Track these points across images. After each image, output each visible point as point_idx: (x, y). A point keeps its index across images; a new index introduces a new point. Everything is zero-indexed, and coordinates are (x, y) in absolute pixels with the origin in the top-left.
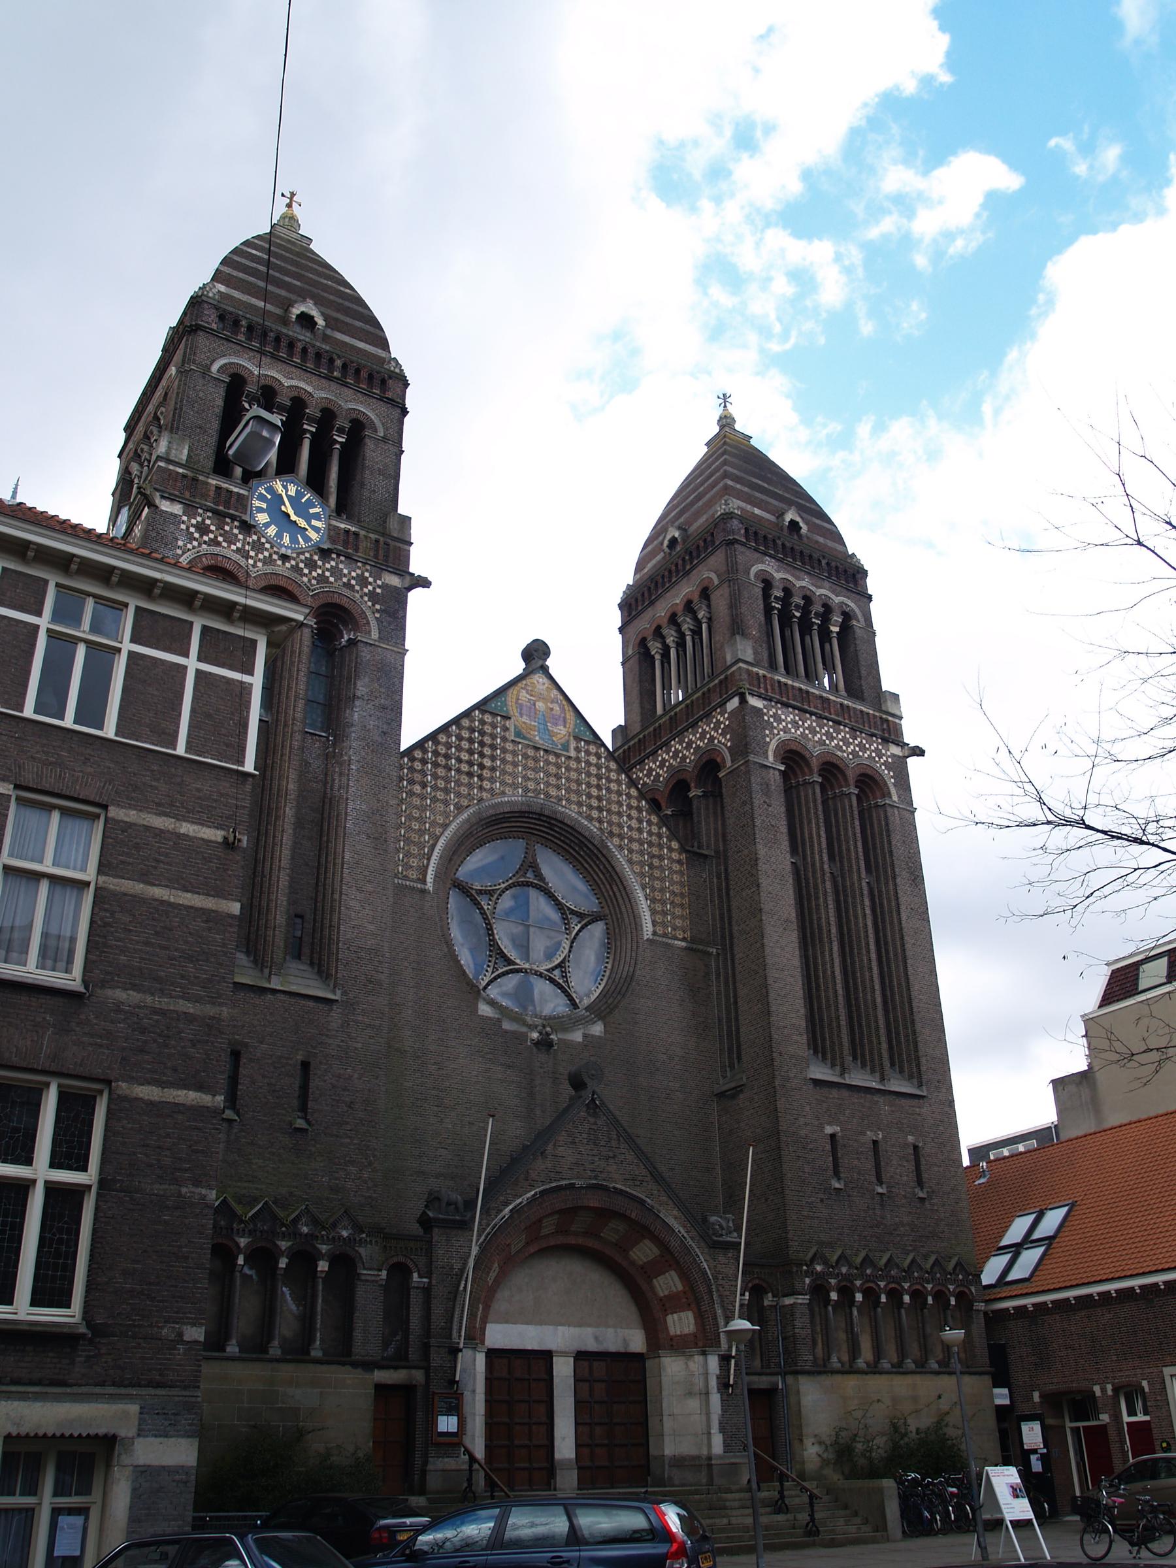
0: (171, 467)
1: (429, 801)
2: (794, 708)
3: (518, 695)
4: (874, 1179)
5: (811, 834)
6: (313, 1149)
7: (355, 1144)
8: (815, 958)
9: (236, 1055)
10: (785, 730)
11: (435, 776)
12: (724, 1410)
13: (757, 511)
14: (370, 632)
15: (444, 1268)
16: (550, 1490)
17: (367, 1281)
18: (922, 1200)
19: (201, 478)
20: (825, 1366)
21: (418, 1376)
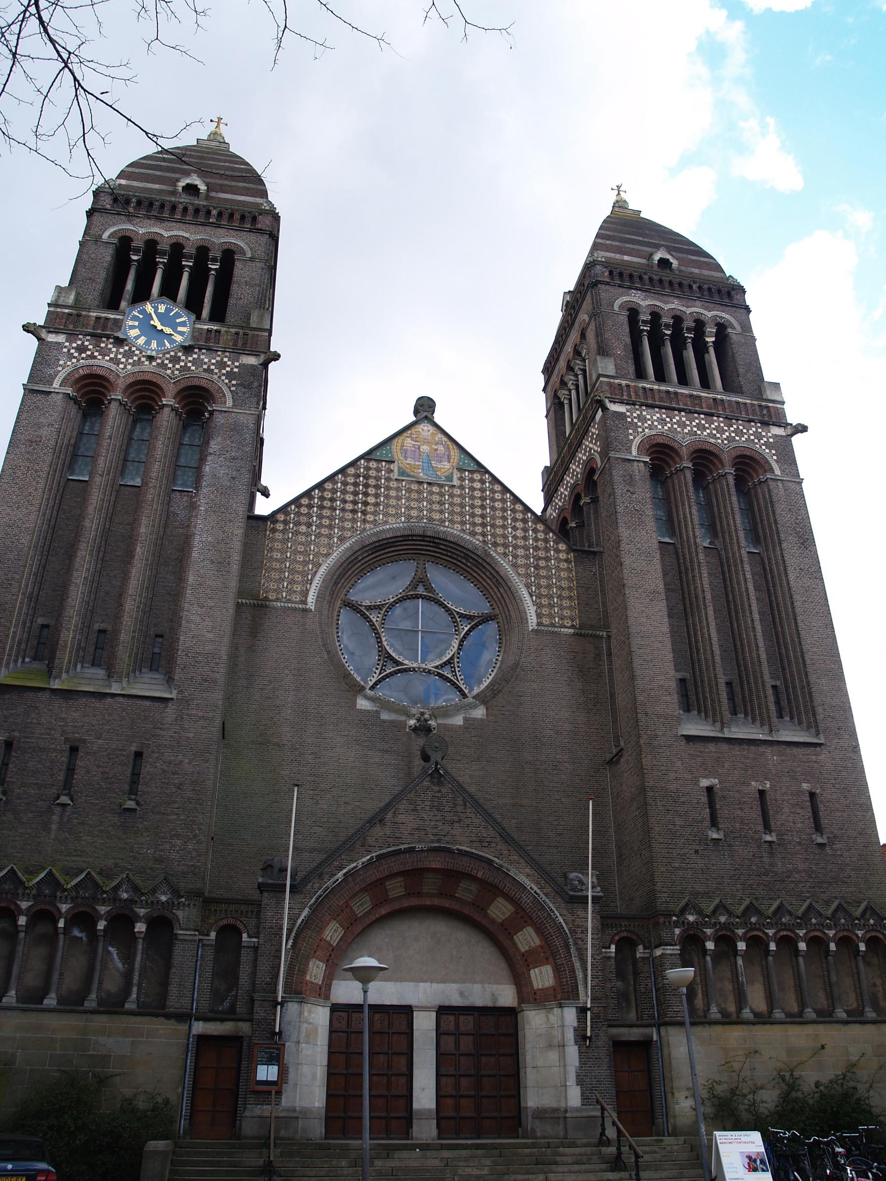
0: (59, 310)
1: (313, 537)
2: (660, 407)
3: (403, 443)
4: (760, 828)
5: (684, 514)
6: (140, 826)
7: (182, 820)
8: (694, 625)
9: (74, 750)
10: (650, 427)
11: (320, 517)
12: (582, 1063)
13: (626, 258)
14: (225, 402)
15: (271, 928)
16: (408, 1139)
17: (185, 940)
18: (821, 846)
19: (84, 313)
20: (705, 1017)
21: (245, 1028)
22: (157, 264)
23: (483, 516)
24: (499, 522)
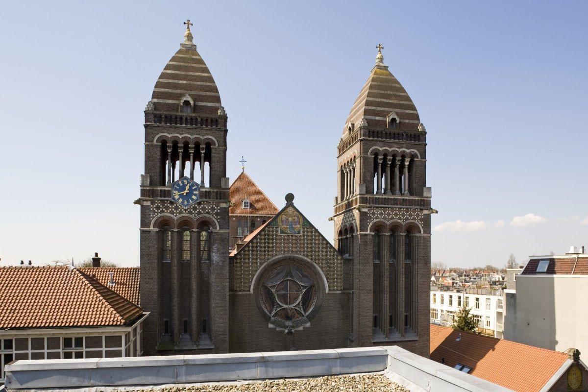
11: (253, 255)
13: (378, 118)
22: (179, 153)
23: (311, 248)
24: (317, 250)
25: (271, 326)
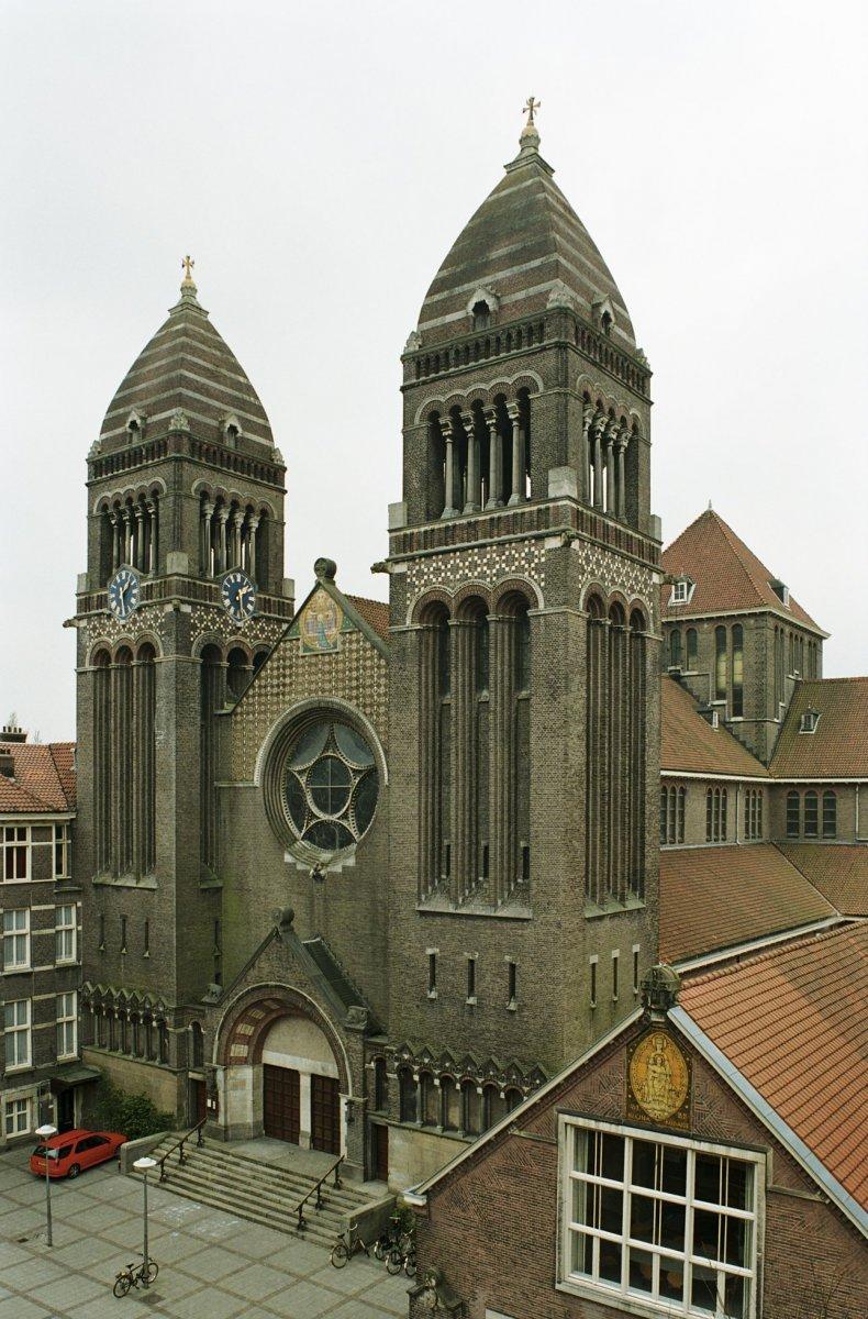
4: (466, 992)
9: (124, 920)
18: (512, 1012)
24: (368, 682)
25: (288, 858)
